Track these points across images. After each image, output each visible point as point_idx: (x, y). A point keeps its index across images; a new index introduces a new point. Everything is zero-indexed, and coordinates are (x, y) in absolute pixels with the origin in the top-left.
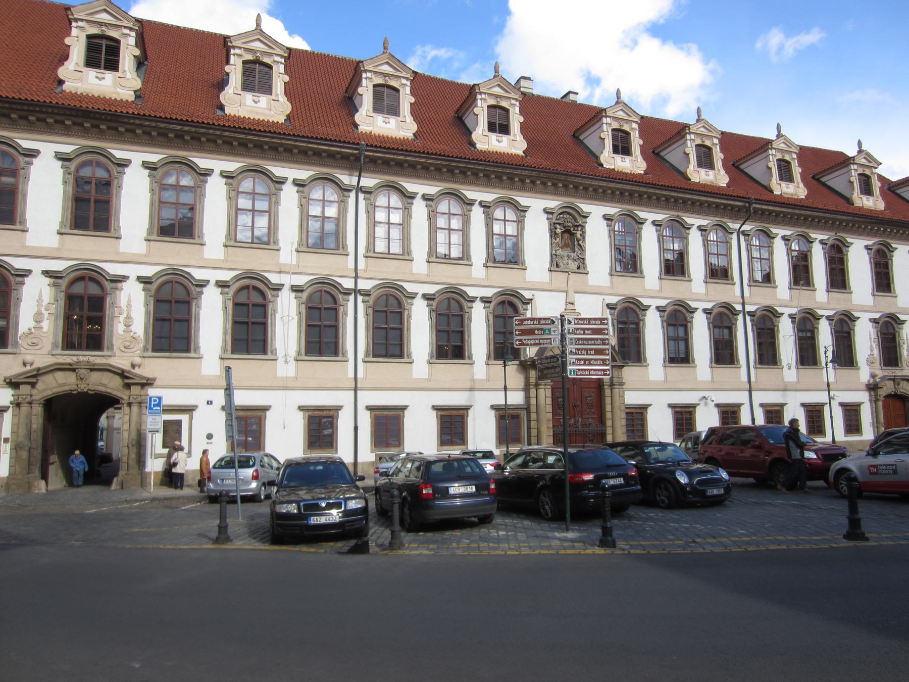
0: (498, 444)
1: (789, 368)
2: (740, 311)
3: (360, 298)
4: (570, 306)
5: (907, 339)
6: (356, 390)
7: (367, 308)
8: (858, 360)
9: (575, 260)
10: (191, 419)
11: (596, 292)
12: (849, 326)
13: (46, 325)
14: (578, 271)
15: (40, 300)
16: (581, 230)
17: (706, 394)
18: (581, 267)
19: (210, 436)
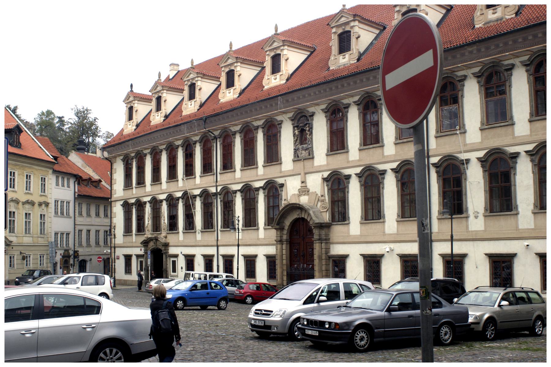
0: (268, 279)
1: (476, 217)
4: (303, 185)
6: (218, 246)
7: (221, 201)
10: (177, 259)
13: (150, 222)
15: (149, 213)
16: (308, 127)
17: (392, 246)
19: (182, 268)
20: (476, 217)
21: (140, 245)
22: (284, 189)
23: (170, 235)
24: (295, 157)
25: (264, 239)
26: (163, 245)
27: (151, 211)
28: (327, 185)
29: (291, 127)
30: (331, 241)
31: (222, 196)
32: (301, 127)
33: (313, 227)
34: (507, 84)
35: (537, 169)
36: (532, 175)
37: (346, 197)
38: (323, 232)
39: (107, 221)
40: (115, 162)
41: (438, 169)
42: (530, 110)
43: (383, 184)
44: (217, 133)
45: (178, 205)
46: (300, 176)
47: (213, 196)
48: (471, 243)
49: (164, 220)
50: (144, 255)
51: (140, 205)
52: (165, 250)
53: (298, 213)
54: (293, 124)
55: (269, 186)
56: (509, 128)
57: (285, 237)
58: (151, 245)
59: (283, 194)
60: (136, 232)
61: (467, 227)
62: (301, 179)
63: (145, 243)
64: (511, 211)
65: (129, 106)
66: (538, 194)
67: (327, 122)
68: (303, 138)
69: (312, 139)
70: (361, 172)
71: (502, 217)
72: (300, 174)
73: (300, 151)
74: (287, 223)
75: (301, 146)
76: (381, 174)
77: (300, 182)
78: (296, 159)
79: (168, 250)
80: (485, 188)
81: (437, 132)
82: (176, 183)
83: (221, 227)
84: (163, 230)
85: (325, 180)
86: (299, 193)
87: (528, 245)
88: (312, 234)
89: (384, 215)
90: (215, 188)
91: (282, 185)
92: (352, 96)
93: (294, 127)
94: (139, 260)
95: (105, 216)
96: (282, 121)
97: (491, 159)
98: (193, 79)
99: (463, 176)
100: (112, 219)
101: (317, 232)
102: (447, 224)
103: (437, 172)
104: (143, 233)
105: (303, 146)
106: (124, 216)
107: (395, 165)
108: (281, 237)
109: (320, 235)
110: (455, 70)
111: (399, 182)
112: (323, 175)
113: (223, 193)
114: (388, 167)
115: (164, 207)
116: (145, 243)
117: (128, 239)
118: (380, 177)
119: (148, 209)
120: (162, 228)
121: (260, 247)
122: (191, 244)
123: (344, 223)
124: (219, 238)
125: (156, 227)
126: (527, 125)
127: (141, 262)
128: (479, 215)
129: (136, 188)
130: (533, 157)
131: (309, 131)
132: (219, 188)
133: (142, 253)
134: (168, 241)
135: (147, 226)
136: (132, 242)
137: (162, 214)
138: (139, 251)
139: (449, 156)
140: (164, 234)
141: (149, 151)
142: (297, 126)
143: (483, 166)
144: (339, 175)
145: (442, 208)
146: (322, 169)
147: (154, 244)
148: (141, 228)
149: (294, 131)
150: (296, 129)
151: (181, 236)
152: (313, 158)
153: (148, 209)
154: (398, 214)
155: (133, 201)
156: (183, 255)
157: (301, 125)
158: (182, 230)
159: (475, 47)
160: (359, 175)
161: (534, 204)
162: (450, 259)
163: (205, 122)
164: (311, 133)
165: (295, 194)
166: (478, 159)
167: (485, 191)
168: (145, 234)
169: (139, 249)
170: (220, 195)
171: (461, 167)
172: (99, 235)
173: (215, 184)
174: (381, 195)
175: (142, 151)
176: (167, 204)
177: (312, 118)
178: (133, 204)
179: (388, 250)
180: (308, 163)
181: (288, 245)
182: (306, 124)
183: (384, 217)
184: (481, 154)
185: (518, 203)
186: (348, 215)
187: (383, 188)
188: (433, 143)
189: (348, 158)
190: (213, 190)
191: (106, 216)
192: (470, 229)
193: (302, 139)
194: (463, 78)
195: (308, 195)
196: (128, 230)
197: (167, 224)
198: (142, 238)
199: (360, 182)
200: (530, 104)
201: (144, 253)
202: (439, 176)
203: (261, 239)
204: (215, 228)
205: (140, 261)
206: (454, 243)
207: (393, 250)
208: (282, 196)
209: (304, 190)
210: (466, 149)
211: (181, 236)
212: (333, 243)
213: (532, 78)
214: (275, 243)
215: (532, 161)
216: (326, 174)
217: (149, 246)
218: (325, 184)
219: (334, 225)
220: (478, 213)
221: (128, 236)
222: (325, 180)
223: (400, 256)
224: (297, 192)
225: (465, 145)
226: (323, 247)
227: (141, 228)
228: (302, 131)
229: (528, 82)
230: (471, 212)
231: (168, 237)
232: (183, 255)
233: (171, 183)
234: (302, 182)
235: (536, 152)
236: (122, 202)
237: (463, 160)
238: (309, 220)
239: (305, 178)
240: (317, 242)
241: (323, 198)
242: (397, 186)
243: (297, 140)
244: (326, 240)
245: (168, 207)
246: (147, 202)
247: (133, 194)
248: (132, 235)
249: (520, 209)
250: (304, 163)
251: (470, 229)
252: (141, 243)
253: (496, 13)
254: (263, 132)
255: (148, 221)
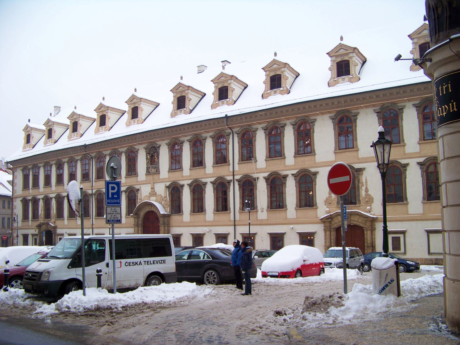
1: (262, 211)
2: (231, 180)
3: (93, 196)
4: (152, 190)
5: (366, 182)
6: (93, 229)
7: (95, 199)
8: (318, 201)
9: (155, 168)
11: (163, 181)
12: (312, 178)
13: (43, 212)
14: (157, 173)
15: (41, 206)
17: (211, 228)
18: (158, 172)
20: (262, 211)
21: (35, 227)
22: (139, 192)
23: (58, 221)
24: (147, 172)
25: (125, 224)
26: (52, 228)
27: (44, 205)
28: (168, 191)
29: (145, 153)
30: (171, 225)
31: (96, 196)
32: (151, 154)
33: (159, 217)
34: (282, 135)
35: (298, 184)
36: (295, 188)
37: (181, 198)
38: (166, 220)
39: (10, 211)
40: (16, 171)
41: (239, 183)
42: (295, 151)
43: (205, 191)
44: (93, 155)
45: (64, 202)
46: (150, 184)
47: (90, 195)
48: (259, 226)
49: (53, 211)
50: (38, 234)
51: (35, 201)
52: (54, 231)
53: (149, 208)
54: (146, 152)
55: (129, 190)
56: (283, 160)
57: (140, 222)
58: (44, 227)
59: (139, 195)
60: (32, 219)
61: (257, 217)
62: (151, 186)
63: (39, 226)
64: (283, 208)
65: (27, 134)
66: (299, 198)
67: (169, 151)
68: (153, 161)
69: (159, 161)
70: (191, 183)
71: (277, 211)
72: (150, 183)
73: (151, 169)
74: (142, 214)
75: (151, 166)
76: (204, 185)
77: (150, 188)
78: (148, 174)
79: (56, 231)
80: (267, 195)
81: (239, 161)
82: (62, 186)
83: (95, 216)
84: (52, 218)
85: (168, 187)
86: (149, 195)
87: (292, 228)
88: (159, 221)
89: (205, 210)
90: (91, 190)
91: (138, 190)
92: (186, 136)
93: (147, 154)
94: (34, 237)
95: (3, 208)
96: (139, 149)
97: (271, 178)
98: (75, 119)
99: (254, 187)
100: (13, 210)
101: (162, 219)
102: (245, 216)
103: (239, 184)
104: (37, 220)
105: (153, 165)
106: (22, 208)
107: (213, 179)
108: (138, 222)
109: (164, 221)
110: (252, 124)
111: (215, 190)
112: (166, 184)
113: (97, 194)
114: (209, 180)
115: (54, 203)
116: (39, 226)
117: (26, 223)
118: (203, 186)
119: (41, 204)
120: (52, 217)
121: (123, 229)
122: (73, 227)
123: (179, 214)
124: (94, 223)
125: (48, 215)
126: (293, 159)
127: (36, 239)
128: (264, 210)
129: (32, 189)
130: (296, 178)
131: (157, 156)
132: (94, 191)
133: (37, 232)
134: (56, 225)
135: (40, 215)
136: (29, 226)
137: (52, 207)
138: (35, 231)
139: (246, 175)
140: (53, 220)
141: (43, 164)
142: (149, 153)
143: (266, 182)
144: (177, 184)
145: (242, 206)
146: (165, 180)
147: (45, 227)
148: (35, 216)
149: (147, 156)
150: (148, 155)
151: (66, 222)
152: (159, 173)
153: (41, 204)
154: (214, 209)
155: (30, 198)
156: (67, 234)
157: (152, 152)
158: (67, 218)
159: (264, 113)
160: (190, 185)
161: (296, 204)
162: (248, 236)
163: (85, 148)
164: (158, 158)
165: (147, 196)
166: (264, 178)
167: (267, 196)
168: (39, 220)
169: (34, 230)
170: (94, 195)
171: (254, 182)
172: (4, 221)
173: (91, 188)
174: (204, 197)
175: (37, 164)
176: (55, 201)
177: (159, 148)
178: (29, 200)
179: (208, 230)
180: (156, 177)
181: (142, 228)
182: (155, 152)
183: (205, 211)
184: (266, 175)
185: (287, 203)
186: (182, 209)
187: (205, 193)
188: (237, 167)
189: (182, 174)
190: (90, 192)
191: (9, 208)
192: (259, 218)
193: (152, 161)
194: (256, 130)
195: (156, 196)
196: (25, 217)
197: (55, 213)
198: (37, 223)
199: (190, 189)
200: (295, 147)
201: (38, 233)
202: (240, 187)
203: (123, 224)
204: (91, 217)
205: (35, 238)
206: (251, 226)
207: (211, 231)
208: (138, 197)
209: (153, 193)
210: (257, 171)
211: (66, 222)
212: (172, 226)
213: (296, 132)
214: (134, 226)
215: (295, 179)
216: (168, 184)
217: (42, 229)
218: (167, 190)
219: (173, 215)
220: (263, 209)
221: (25, 222)
222: (168, 187)
223: (215, 235)
224: (148, 195)
225: (256, 169)
226: (166, 229)
227: (35, 216)
228: (152, 156)
229: (294, 134)
230: (259, 208)
231: (56, 222)
232: (67, 234)
233: (59, 186)
234: (152, 188)
235: (298, 175)
236: (21, 199)
237: (255, 178)
238: (156, 212)
239: (154, 186)
240: (162, 226)
241: (165, 199)
242: (214, 193)
243: (148, 162)
244: (167, 224)
245: (56, 202)
246: (41, 199)
247: (29, 193)
248: (29, 221)
249: (288, 207)
250: (153, 176)
251: (259, 218)
252: (37, 226)
253: (276, 93)
254: (125, 155)
255: (41, 211)
